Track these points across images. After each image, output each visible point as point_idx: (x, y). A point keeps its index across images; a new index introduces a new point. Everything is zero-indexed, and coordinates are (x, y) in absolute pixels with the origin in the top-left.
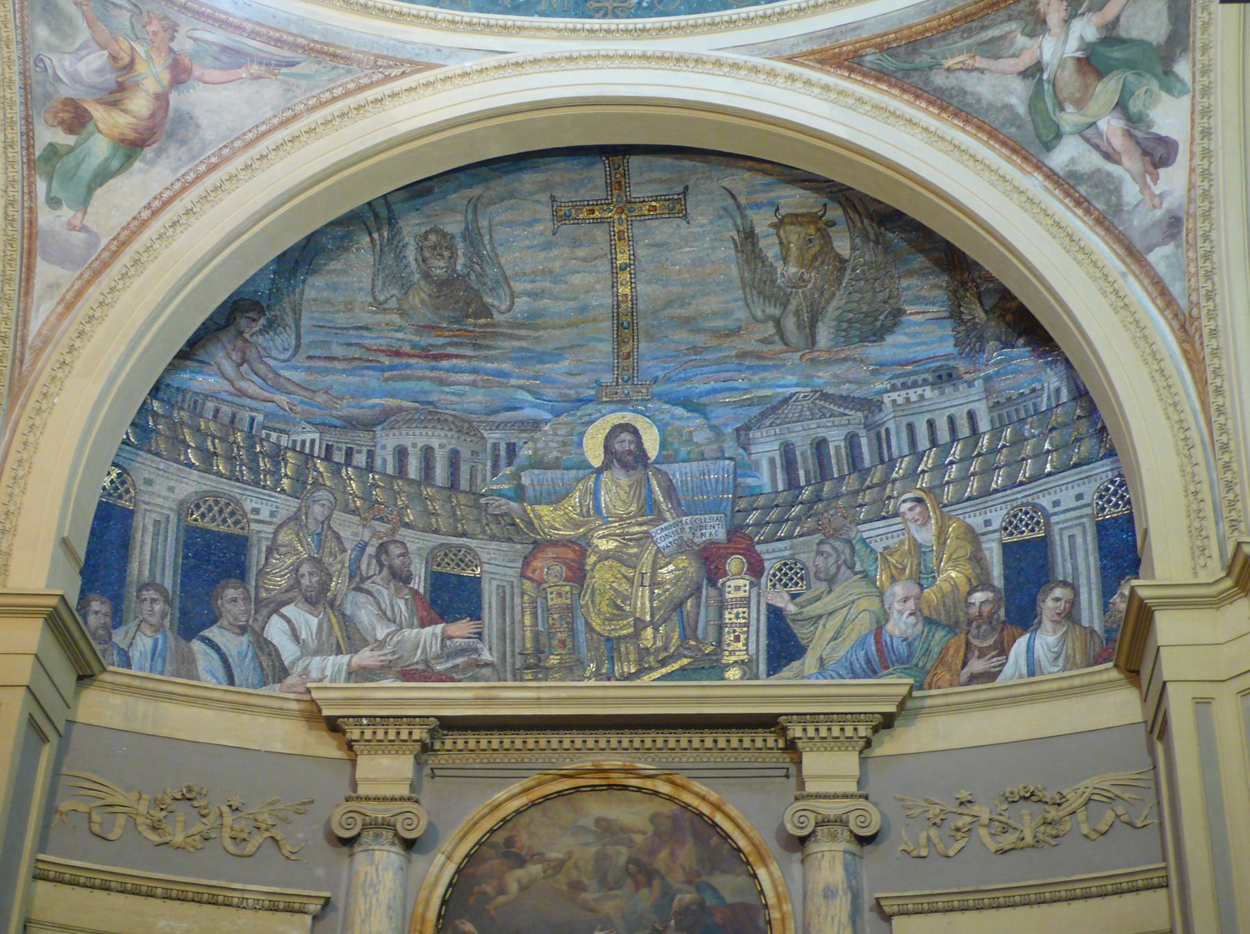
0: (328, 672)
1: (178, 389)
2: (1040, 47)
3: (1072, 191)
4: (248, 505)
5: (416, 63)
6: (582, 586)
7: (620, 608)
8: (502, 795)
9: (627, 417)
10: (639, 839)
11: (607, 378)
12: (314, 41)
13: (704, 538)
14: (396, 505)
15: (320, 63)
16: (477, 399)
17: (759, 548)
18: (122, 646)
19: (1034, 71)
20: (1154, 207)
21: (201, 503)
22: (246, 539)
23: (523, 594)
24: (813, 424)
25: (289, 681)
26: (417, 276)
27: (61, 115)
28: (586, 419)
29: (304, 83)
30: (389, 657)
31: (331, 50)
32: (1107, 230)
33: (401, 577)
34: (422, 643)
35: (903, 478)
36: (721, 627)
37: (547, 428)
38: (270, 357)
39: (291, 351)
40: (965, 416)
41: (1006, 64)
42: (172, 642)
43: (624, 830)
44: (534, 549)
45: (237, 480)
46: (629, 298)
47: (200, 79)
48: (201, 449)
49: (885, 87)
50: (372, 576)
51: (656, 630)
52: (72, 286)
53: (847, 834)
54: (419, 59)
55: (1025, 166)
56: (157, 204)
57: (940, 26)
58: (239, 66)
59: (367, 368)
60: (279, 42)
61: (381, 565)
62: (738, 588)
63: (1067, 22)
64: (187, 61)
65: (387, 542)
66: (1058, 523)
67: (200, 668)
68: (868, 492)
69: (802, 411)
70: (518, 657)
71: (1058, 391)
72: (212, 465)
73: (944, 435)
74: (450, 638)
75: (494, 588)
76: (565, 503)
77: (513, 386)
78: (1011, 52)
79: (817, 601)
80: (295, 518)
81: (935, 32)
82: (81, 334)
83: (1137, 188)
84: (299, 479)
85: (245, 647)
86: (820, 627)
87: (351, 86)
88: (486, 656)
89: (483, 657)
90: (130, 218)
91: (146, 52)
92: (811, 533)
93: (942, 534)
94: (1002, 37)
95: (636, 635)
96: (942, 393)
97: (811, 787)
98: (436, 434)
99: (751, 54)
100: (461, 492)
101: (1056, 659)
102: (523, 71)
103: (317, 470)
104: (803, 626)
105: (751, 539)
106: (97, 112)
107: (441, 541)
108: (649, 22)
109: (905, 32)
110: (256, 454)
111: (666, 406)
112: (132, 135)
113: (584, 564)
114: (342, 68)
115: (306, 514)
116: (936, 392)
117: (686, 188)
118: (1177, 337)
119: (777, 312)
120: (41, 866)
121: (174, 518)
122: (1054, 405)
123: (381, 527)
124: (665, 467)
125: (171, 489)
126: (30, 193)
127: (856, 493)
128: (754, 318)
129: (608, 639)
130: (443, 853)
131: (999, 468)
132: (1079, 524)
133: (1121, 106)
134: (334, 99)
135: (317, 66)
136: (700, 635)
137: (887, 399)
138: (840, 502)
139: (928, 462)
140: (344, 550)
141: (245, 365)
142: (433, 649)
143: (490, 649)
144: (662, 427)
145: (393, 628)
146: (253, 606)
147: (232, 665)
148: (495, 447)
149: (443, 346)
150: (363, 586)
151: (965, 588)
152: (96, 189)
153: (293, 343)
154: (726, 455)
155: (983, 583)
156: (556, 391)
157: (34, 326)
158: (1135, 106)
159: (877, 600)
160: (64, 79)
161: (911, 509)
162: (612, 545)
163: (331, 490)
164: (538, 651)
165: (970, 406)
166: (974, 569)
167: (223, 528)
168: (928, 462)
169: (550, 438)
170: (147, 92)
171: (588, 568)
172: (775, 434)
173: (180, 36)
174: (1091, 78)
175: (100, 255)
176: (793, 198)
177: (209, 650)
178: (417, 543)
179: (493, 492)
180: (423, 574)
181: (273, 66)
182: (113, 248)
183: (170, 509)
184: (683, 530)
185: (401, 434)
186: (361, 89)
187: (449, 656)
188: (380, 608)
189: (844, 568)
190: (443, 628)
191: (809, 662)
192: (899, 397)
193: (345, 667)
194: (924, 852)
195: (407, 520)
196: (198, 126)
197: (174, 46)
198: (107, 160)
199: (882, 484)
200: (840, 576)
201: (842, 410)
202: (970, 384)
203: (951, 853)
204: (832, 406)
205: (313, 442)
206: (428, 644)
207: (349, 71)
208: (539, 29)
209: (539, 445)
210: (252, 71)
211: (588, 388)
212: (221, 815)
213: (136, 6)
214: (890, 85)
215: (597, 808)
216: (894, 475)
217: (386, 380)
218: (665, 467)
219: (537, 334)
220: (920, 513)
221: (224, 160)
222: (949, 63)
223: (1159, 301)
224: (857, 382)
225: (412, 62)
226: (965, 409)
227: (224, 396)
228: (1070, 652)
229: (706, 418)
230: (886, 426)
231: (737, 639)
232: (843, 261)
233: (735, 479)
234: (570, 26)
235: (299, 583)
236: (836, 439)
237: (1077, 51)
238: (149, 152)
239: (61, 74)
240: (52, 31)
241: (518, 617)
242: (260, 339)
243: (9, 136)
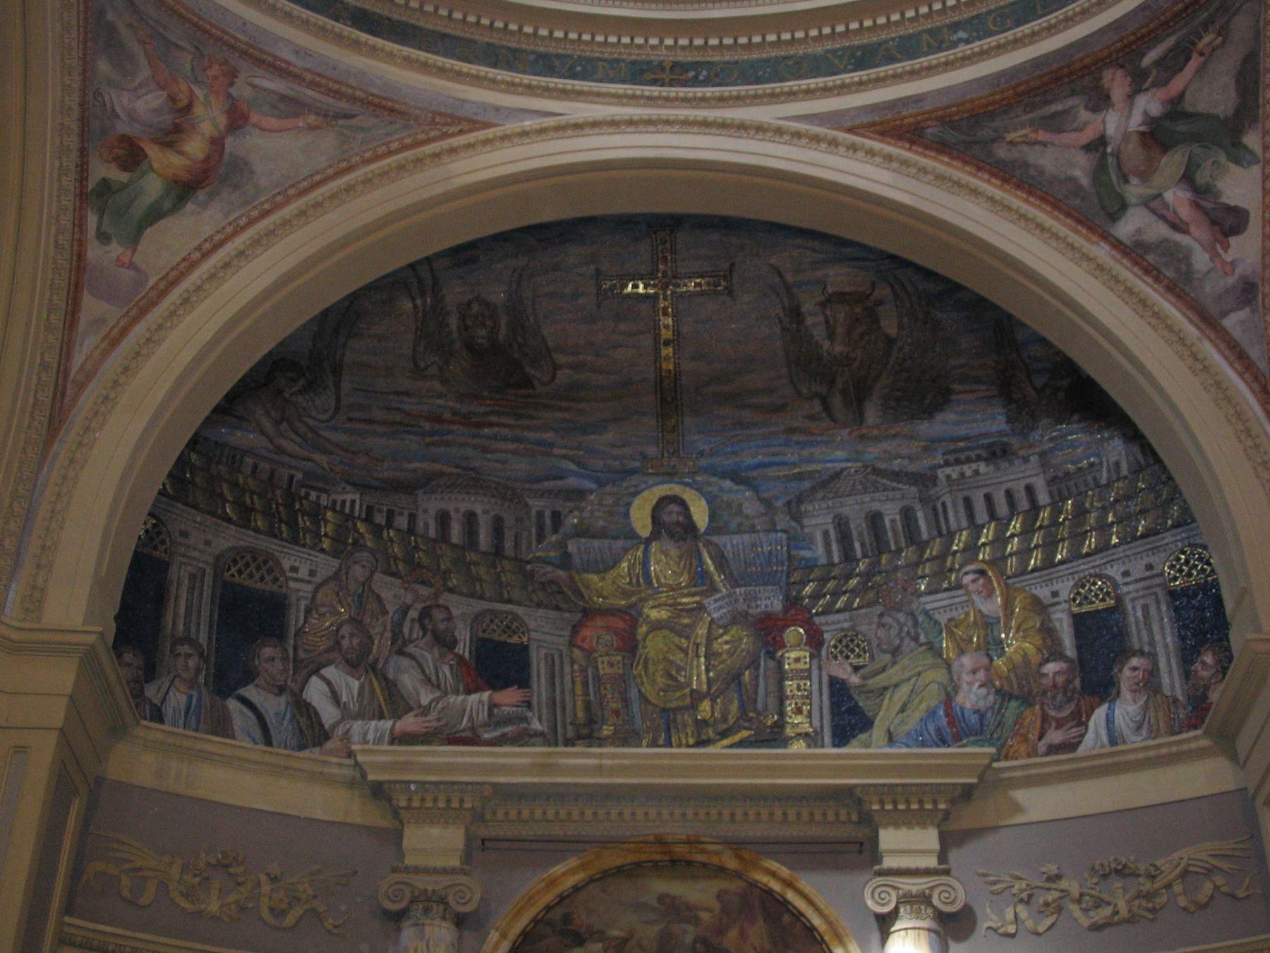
0: (370, 736)
1: (216, 443)
2: (1104, 122)
3: (1139, 260)
4: (286, 564)
6: (634, 656)
7: (675, 679)
8: (558, 869)
9: (675, 489)
10: (705, 916)
11: (652, 451)
12: (372, 95)
13: (759, 610)
14: (439, 569)
15: (377, 117)
16: (520, 466)
17: (817, 620)
18: (156, 701)
20: (1226, 273)
21: (238, 558)
22: (285, 597)
23: (573, 662)
24: (867, 498)
25: (330, 745)
26: (458, 345)
27: (116, 151)
28: (632, 490)
29: (360, 136)
30: (434, 724)
31: (390, 104)
32: (1179, 297)
33: (445, 642)
34: (468, 711)
35: (964, 550)
36: (782, 700)
37: (592, 497)
38: (310, 416)
39: (331, 412)
40: (1022, 489)
41: (1070, 138)
42: (206, 699)
43: (689, 907)
44: (583, 617)
45: (275, 536)
46: (673, 373)
47: (255, 126)
48: (237, 504)
49: (946, 159)
50: (415, 640)
51: (713, 701)
52: (118, 323)
53: (930, 910)
54: (474, 118)
55: (1090, 236)
56: (207, 246)
57: (1002, 100)
58: (297, 115)
59: (408, 432)
60: (338, 94)
61: (424, 628)
62: (797, 660)
63: (1131, 97)
64: (245, 107)
65: (430, 607)
66: (1128, 593)
67: (235, 728)
68: (928, 564)
69: (854, 485)
70: (570, 728)
71: (1117, 464)
72: (250, 521)
73: (1002, 509)
74: (496, 705)
75: (542, 656)
76: (613, 573)
77: (556, 456)
78: (1075, 125)
79: (881, 672)
80: (336, 577)
81: (997, 106)
82: (126, 370)
83: (1207, 256)
84: (338, 539)
85: (283, 707)
86: (886, 701)
87: (408, 141)
88: (536, 725)
89: (533, 726)
90: (179, 259)
91: (206, 96)
92: (870, 604)
93: (1008, 605)
94: (1065, 112)
95: (694, 706)
96: (998, 469)
97: (889, 862)
98: (479, 499)
99: (812, 123)
100: (507, 558)
101: (1139, 728)
102: (582, 133)
103: (357, 530)
104: (868, 698)
105: (810, 611)
106: (153, 152)
107: (486, 607)
108: (709, 91)
109: (968, 106)
110: (295, 512)
111: (714, 479)
112: (185, 177)
113: (635, 635)
115: (347, 573)
116: (991, 467)
117: (732, 265)
118: (1259, 401)
119: (823, 389)
120: (67, 929)
121: (209, 570)
122: (1115, 478)
123: (424, 591)
124: (715, 539)
125: (208, 543)
126: (81, 226)
127: (917, 565)
128: (800, 395)
129: (664, 710)
130: (497, 930)
131: (1063, 540)
132: (1151, 594)
133: (1188, 178)
134: (390, 153)
135: (375, 121)
136: (760, 706)
137: (941, 474)
138: (899, 574)
139: (987, 535)
140: (385, 612)
141: (285, 424)
142: (481, 717)
143: (540, 719)
144: (711, 500)
145: (438, 694)
146: (291, 665)
147: (269, 725)
148: (540, 515)
149: (486, 414)
150: (406, 650)
151: (1035, 658)
152: (146, 228)
153: (333, 404)
154: (779, 528)
155: (1055, 653)
156: (601, 463)
157: (78, 360)
158: (1202, 177)
159: (944, 671)
160: (121, 115)
161: (974, 581)
162: (663, 614)
163: (372, 552)
164: (591, 721)
165: (1028, 481)
166: (1044, 639)
167: (259, 586)
168: (987, 535)
169: (596, 507)
170: (203, 135)
171: (639, 638)
172: (828, 508)
173: (239, 81)
175: (147, 293)
176: (839, 277)
177: (245, 710)
178: (461, 608)
179: (539, 560)
180: (468, 639)
182: (162, 285)
183: (207, 563)
184: (736, 601)
185: (443, 498)
187: (498, 724)
188: (423, 671)
189: (907, 641)
190: (490, 696)
191: (878, 732)
192: (954, 472)
193: (388, 732)
194: (1012, 929)
195: (450, 584)
196: (252, 172)
197: (233, 91)
199: (942, 557)
200: (904, 648)
201: (894, 484)
202: (1026, 460)
203: (1041, 929)
204: (885, 481)
205: (353, 502)
206: (474, 714)
207: (406, 127)
208: (598, 94)
209: (586, 514)
210: (309, 121)
211: (634, 460)
212: (259, 884)
213: (197, 48)
214: (952, 157)
215: (661, 886)
216: (955, 548)
217: (428, 445)
218: (715, 539)
219: (580, 406)
220: (984, 585)
221: (277, 207)
222: (1010, 137)
223: (1236, 365)
224: (911, 458)
226: (1022, 484)
227: (264, 453)
228: (1152, 721)
229: (757, 492)
230: (943, 499)
231: (799, 711)
232: (891, 341)
233: (789, 552)
234: (630, 92)
235: (338, 643)
236: (891, 513)
237: (1140, 125)
238: (201, 195)
239: (119, 111)
241: (568, 686)
242: (300, 399)
243: (65, 164)
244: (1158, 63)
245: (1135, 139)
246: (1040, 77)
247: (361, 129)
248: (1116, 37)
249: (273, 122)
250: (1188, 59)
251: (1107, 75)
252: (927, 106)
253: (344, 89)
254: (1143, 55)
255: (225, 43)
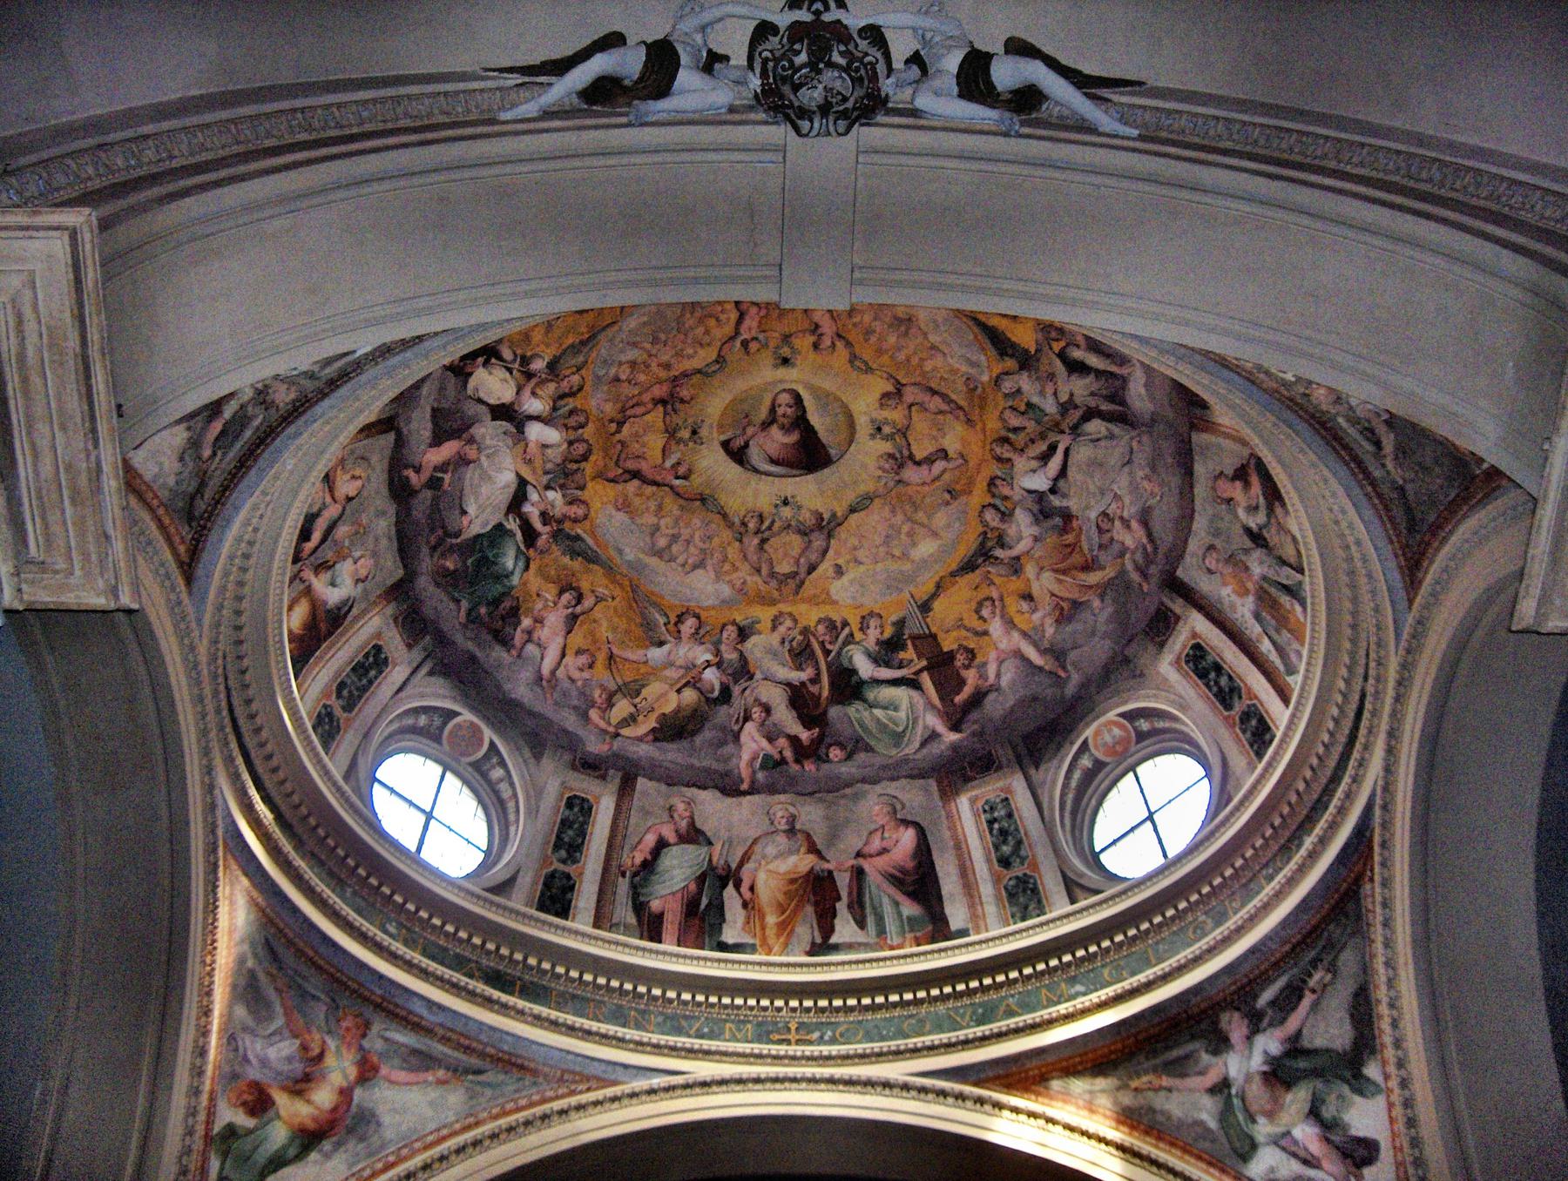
5: (603, 1080)
19: (1222, 1087)
29: (489, 1092)
31: (519, 1061)
41: (1194, 1082)
60: (467, 1050)
63: (1249, 1038)
64: (375, 1059)
87: (536, 1098)
91: (337, 1047)
94: (1187, 1057)
106: (281, 1099)
108: (834, 1049)
112: (311, 1125)
114: (528, 1080)
133: (1314, 1113)
134: (519, 1109)
158: (1328, 1112)
174: (1280, 1090)
181: (458, 1071)
186: (544, 1101)
196: (379, 1124)
197: (366, 1043)
198: (285, 1148)
208: (725, 1054)
225: (598, 1079)
238: (327, 1145)
239: (251, 1056)
240: (250, 1012)
244: (1273, 1003)
245: (1257, 1079)
246: (1159, 1024)
247: (489, 1085)
248: (1229, 981)
249: (402, 1076)
250: (1300, 998)
251: (1225, 1017)
252: (1050, 1058)
253: (474, 1045)
254: (1256, 997)
255: (360, 996)
